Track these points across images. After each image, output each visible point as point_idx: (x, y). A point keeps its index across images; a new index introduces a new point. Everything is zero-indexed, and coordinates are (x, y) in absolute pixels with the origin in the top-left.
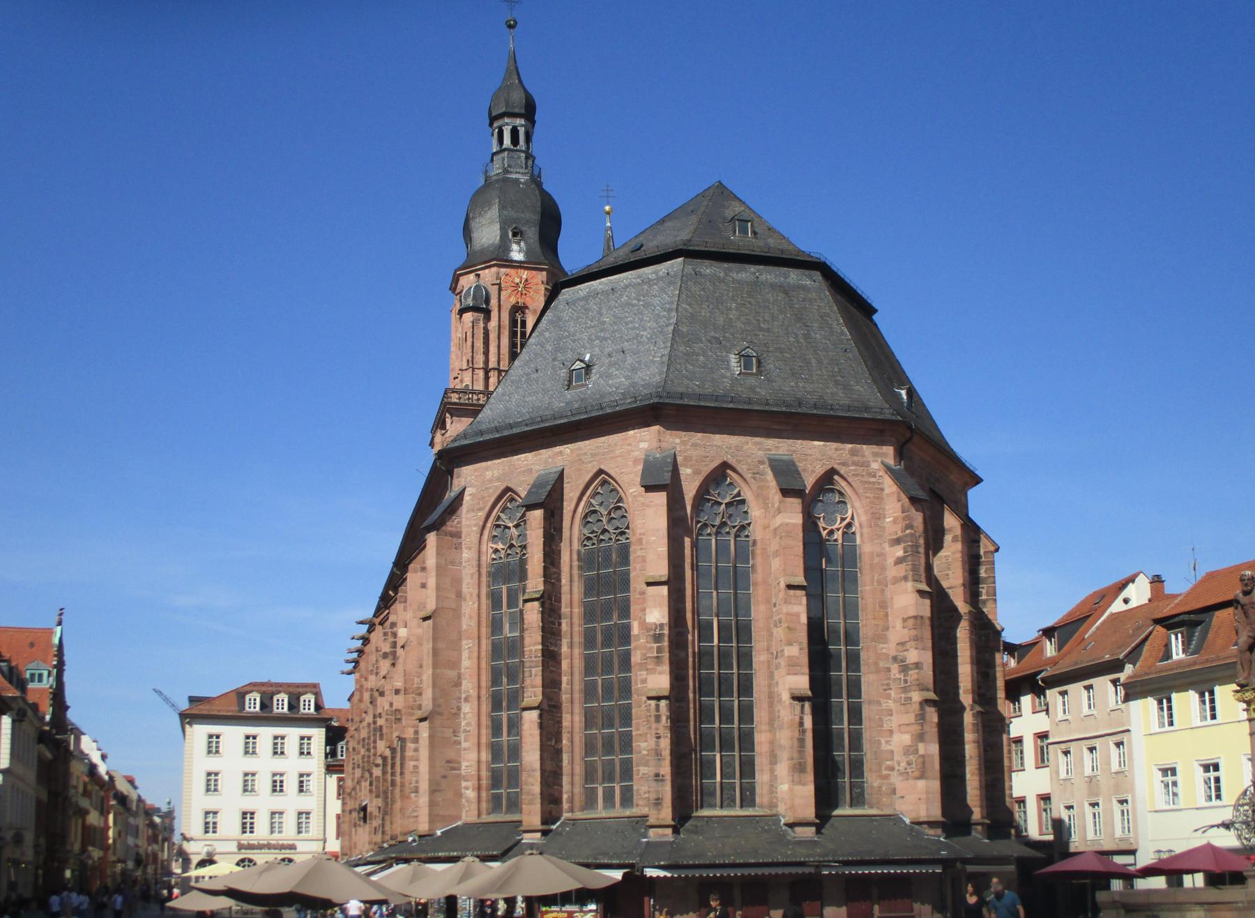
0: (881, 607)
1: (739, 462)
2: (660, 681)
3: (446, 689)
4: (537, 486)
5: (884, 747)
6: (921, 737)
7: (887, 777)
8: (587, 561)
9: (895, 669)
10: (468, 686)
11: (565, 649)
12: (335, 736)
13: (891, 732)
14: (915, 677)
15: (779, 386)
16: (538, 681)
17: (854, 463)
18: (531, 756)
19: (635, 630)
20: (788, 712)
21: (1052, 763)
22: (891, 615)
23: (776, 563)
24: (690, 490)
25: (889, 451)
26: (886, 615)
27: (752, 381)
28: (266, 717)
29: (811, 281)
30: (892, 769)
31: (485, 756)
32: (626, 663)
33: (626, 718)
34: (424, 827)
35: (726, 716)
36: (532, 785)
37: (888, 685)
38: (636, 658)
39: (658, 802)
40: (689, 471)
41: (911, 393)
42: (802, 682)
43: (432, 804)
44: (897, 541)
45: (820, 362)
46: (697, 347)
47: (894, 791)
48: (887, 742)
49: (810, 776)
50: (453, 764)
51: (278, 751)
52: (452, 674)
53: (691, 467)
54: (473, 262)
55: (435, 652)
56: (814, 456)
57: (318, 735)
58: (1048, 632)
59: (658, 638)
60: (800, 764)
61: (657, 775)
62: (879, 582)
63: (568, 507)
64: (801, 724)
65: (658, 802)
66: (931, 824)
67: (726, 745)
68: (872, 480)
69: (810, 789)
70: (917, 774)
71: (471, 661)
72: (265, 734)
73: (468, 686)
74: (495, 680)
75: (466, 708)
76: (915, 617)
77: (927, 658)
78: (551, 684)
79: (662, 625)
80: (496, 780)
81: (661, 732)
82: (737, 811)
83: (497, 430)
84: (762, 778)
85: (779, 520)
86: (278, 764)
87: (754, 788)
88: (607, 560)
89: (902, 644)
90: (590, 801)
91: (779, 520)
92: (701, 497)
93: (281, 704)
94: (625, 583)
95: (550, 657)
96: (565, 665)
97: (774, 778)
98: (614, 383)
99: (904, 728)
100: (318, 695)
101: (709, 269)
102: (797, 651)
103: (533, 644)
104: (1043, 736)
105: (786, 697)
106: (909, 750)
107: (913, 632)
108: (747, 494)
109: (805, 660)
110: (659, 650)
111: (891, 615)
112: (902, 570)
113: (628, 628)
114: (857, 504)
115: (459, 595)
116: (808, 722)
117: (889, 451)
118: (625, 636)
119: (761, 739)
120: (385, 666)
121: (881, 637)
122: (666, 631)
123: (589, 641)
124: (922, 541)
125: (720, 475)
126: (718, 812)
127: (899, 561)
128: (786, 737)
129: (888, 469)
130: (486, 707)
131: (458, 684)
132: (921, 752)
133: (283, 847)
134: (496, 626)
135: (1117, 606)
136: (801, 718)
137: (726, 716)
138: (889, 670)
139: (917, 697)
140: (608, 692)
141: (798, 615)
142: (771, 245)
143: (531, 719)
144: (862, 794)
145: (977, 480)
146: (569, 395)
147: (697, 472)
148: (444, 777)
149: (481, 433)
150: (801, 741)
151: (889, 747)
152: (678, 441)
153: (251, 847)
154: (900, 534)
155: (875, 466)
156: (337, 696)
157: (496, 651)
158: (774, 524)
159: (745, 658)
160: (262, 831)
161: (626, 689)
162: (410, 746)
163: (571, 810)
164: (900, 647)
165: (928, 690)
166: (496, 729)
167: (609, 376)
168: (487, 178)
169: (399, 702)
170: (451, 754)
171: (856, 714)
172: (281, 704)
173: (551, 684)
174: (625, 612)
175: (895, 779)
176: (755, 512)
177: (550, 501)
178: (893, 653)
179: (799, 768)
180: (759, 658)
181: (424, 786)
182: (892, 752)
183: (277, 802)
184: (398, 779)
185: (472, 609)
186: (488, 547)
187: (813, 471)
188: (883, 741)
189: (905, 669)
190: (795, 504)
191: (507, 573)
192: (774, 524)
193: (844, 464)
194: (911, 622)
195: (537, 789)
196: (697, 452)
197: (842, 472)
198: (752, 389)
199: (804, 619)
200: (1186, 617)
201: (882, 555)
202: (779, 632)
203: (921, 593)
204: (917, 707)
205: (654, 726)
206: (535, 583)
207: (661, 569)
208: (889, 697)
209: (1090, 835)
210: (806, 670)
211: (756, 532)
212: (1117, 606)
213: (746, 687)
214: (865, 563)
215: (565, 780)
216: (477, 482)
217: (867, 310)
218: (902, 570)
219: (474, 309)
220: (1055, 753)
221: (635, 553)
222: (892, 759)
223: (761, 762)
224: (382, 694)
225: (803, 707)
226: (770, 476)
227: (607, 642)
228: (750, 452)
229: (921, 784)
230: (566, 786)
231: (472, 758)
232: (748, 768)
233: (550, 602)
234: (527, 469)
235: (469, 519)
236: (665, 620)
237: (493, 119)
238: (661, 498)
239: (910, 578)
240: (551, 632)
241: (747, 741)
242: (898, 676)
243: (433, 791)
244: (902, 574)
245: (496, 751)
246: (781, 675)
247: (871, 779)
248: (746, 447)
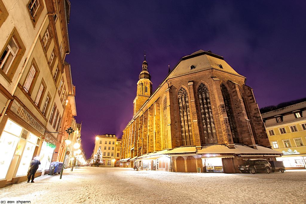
9: (255, 118)
44: (250, 96)
59: (223, 107)
61: (229, 134)
79: (223, 105)
81: (228, 125)
122: (224, 106)
148: (173, 137)
162: (157, 134)
205: (226, 124)
242: (255, 119)
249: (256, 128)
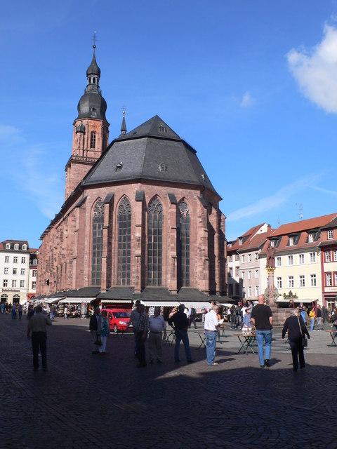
2: (139, 252)
3: (81, 250)
4: (107, 197)
6: (204, 269)
8: (120, 218)
10: (87, 250)
11: (113, 242)
12: (33, 257)
15: (173, 175)
16: (106, 250)
18: (104, 270)
19: (132, 237)
20: (170, 261)
22: (198, 235)
23: (169, 222)
24: (148, 201)
25: (199, 192)
27: (164, 172)
28: (12, 250)
29: (180, 145)
31: (91, 269)
32: (129, 246)
33: (129, 261)
34: (74, 288)
35: (155, 262)
36: (104, 278)
38: (132, 245)
39: (137, 284)
41: (206, 176)
42: (175, 253)
43: (76, 282)
46: (150, 163)
47: (197, 282)
49: (176, 278)
50: (82, 271)
51: (15, 260)
52: (83, 246)
54: (80, 117)
55: (78, 240)
56: (179, 193)
57: (27, 257)
58: (240, 238)
59: (138, 240)
63: (115, 203)
65: (137, 284)
66: (206, 291)
67: (155, 269)
69: (176, 281)
71: (88, 243)
72: (12, 256)
73: (87, 250)
74: (94, 249)
75: (86, 256)
78: (110, 251)
80: (93, 276)
82: (157, 286)
83: (97, 181)
84: (163, 278)
85: (170, 211)
86: (15, 266)
88: (125, 219)
90: (119, 282)
91: (170, 211)
92: (150, 203)
93: (17, 246)
94: (130, 224)
95: (110, 244)
96: (113, 246)
98: (128, 171)
100: (27, 244)
101: (154, 141)
102: (174, 245)
103: (105, 240)
104: (238, 268)
106: (201, 272)
108: (162, 203)
111: (198, 235)
112: (201, 225)
113: (130, 237)
115: (85, 225)
116: (176, 264)
117: (199, 192)
118: (129, 239)
120: (57, 241)
121: (195, 242)
123: (120, 239)
125: (155, 198)
126: (152, 287)
127: (201, 222)
128: (170, 268)
129: (199, 198)
130: (91, 256)
131: (84, 250)
133: (15, 291)
134: (94, 234)
135: (259, 232)
137: (155, 262)
139: (203, 258)
140: (124, 253)
142: (172, 136)
143: (104, 260)
144: (188, 283)
146: (116, 173)
149: (92, 182)
150: (174, 269)
153: (6, 291)
156: (35, 244)
157: (94, 241)
158: (169, 211)
159: (160, 246)
160: (9, 286)
161: (129, 253)
163: (114, 284)
166: (94, 262)
167: (128, 169)
168: (85, 92)
169: (64, 252)
170: (81, 268)
171: (188, 262)
172: (17, 246)
173: (110, 251)
174: (130, 232)
175: (197, 280)
176: (164, 208)
177: (110, 201)
179: (173, 276)
180: (164, 246)
181: (74, 277)
183: (14, 277)
184: (63, 274)
185: (88, 229)
186: (93, 213)
189: (201, 251)
190: (174, 206)
191: (98, 220)
192: (169, 211)
195: (105, 279)
196: (150, 191)
198: (164, 175)
199: (176, 237)
202: (169, 240)
203: (205, 231)
206: (106, 224)
207: (140, 222)
209: (249, 296)
211: (164, 213)
212: (259, 232)
213: (160, 254)
214: (192, 222)
215: (112, 276)
216: (91, 194)
217: (194, 152)
218: (201, 225)
219: (80, 132)
220: (241, 272)
221: (133, 217)
223: (163, 274)
224: (56, 249)
226: (168, 198)
227: (125, 240)
228: (163, 191)
230: (112, 278)
231: (87, 270)
232: (160, 275)
233: (110, 229)
234: (104, 192)
235: (88, 205)
236: (140, 236)
237: (87, 75)
238: (140, 203)
240: (110, 237)
241: (160, 268)
243: (77, 278)
245: (93, 268)
246: (169, 252)
247: (191, 280)
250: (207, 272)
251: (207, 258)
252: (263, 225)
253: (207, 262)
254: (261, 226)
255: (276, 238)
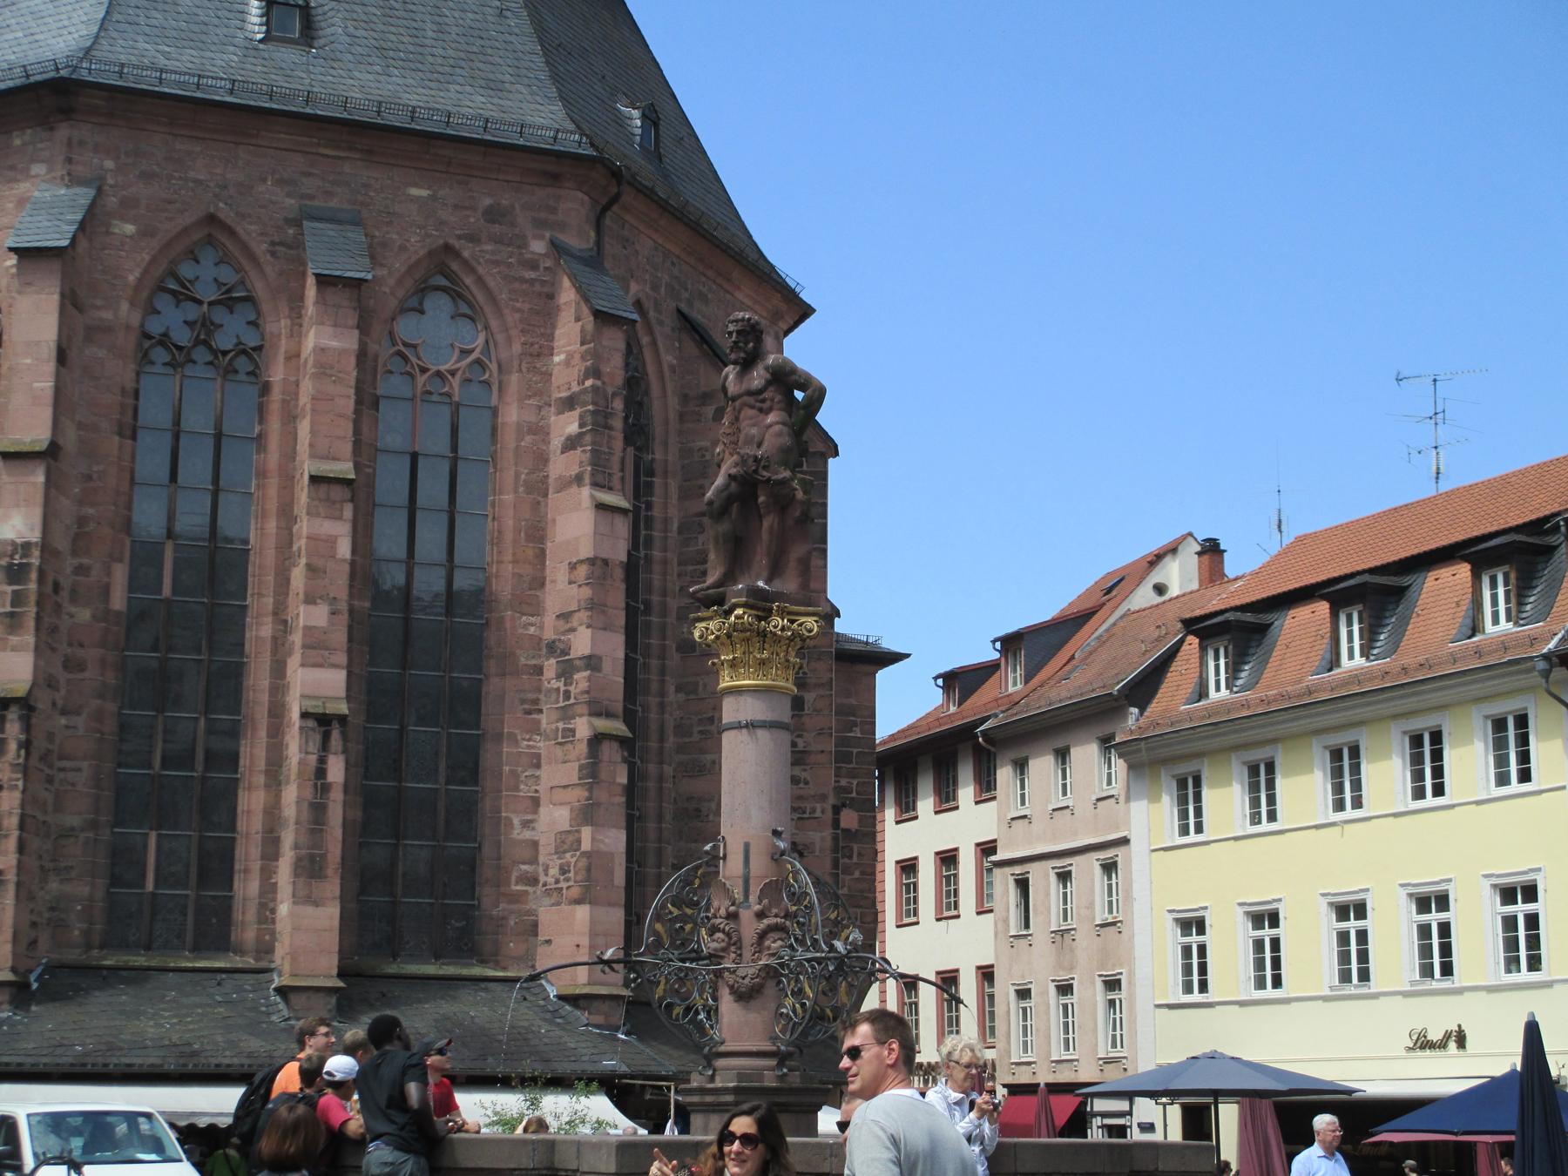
0: (529, 538)
1: (243, 216)
5: (519, 833)
6: (588, 814)
7: (519, 898)
9: (550, 666)
13: (536, 802)
14: (584, 685)
17: (497, 240)
21: (997, 904)
26: (542, 555)
27: (288, 56)
30: (534, 881)
37: (536, 701)
40: (130, 228)
44: (569, 403)
45: (441, 30)
47: (534, 929)
48: (526, 824)
49: (332, 887)
53: (134, 221)
60: (312, 858)
62: (530, 488)
64: (321, 772)
68: (533, 275)
70: (575, 892)
76: (592, 561)
77: (614, 647)
79: (27, 546)
87: (230, 908)
89: (565, 616)
97: (269, 889)
99: (560, 795)
104: (987, 848)
105: (295, 714)
107: (587, 592)
109: (340, 637)
110: (18, 599)
114: (494, 323)
116: (336, 771)
119: (251, 802)
122: (35, 560)
124: (618, 405)
127: (571, 444)
132: (586, 845)
136: (322, 761)
138: (539, 670)
139: (583, 727)
141: (332, 541)
145: (805, 312)
147: (146, 232)
151: (527, 834)
152: (109, 164)
154: (576, 388)
155: (538, 247)
164: (561, 623)
165: (609, 715)
178: (549, 635)
179: (309, 868)
182: (535, 844)
187: (403, 248)
188: (516, 822)
189: (566, 672)
193: (472, 238)
194: (583, 571)
197: (466, 254)
200: (1230, 616)
201: (540, 431)
204: (582, 748)
208: (535, 729)
210: (342, 658)
222: (534, 861)
223: (248, 853)
225: (326, 738)
229: (582, 913)
232: (217, 865)
236: (35, 536)
239: (587, 480)
242: (555, 684)
244: (575, 470)
248: (261, 188)
249: (525, 790)
250: (616, 840)
251: (618, 727)
252: (1172, 550)
253: (610, 752)
254: (1156, 559)
255: (1240, 631)
